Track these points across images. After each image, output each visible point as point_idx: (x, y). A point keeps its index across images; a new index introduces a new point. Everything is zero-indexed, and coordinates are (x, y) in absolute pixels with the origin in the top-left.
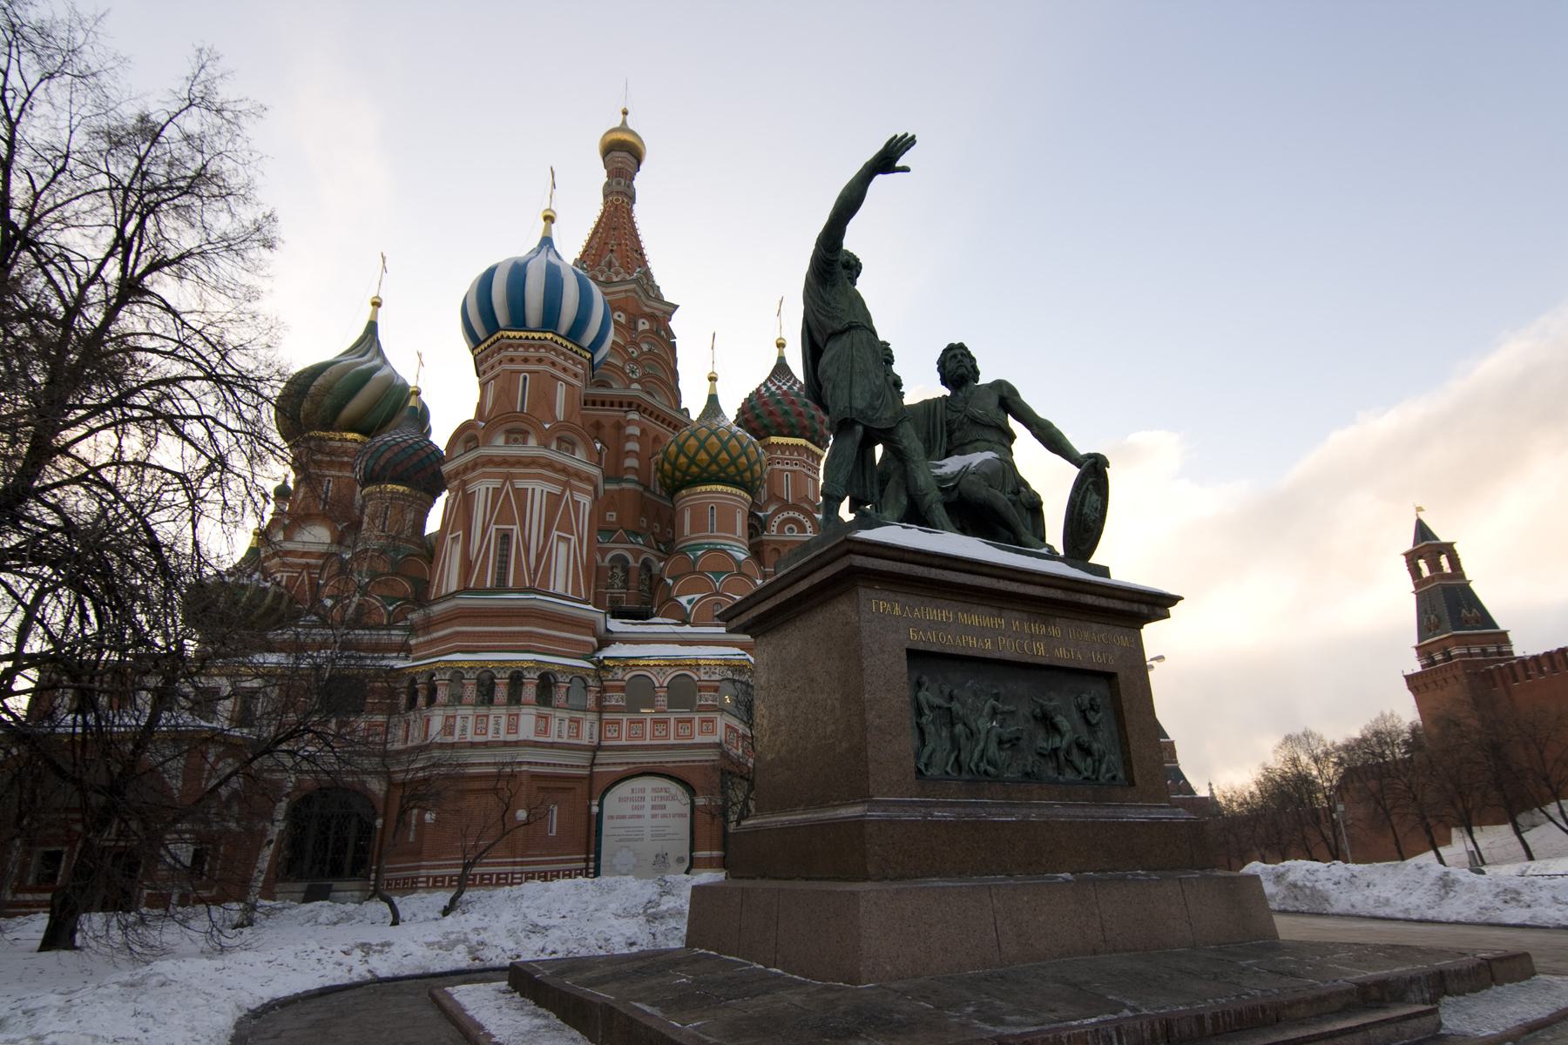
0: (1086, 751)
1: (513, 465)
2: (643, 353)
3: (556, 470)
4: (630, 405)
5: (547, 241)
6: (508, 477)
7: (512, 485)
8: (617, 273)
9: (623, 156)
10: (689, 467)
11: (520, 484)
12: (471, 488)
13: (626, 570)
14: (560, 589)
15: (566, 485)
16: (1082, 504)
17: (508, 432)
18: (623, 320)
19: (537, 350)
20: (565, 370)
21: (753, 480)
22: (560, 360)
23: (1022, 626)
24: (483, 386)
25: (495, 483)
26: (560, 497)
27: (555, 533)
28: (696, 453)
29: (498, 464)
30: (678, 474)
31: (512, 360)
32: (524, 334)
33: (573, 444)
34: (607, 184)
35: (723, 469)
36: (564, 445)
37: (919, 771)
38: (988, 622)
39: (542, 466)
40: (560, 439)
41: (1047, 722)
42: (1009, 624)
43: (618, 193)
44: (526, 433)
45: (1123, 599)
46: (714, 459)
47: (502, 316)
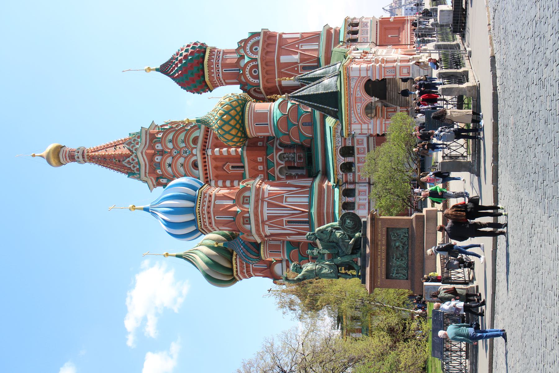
0: (402, 239)
1: (258, 222)
2: (174, 148)
3: (258, 206)
4: (204, 154)
5: (146, 210)
7: (266, 221)
8: (133, 160)
9: (60, 156)
10: (239, 137)
11: (266, 218)
12: (268, 234)
13: (285, 153)
14: (306, 200)
15: (263, 201)
17: (244, 224)
19: (204, 214)
20: (210, 201)
21: (239, 105)
22: (206, 204)
25: (266, 227)
26: (269, 203)
27: (284, 204)
28: (232, 135)
30: (241, 140)
31: (210, 223)
32: (199, 221)
33: (244, 197)
35: (238, 122)
36: (245, 202)
37: (407, 279)
38: (379, 260)
39: (258, 211)
40: (243, 203)
41: (397, 247)
43: (83, 157)
44: (244, 218)
46: (234, 127)
47: (193, 228)
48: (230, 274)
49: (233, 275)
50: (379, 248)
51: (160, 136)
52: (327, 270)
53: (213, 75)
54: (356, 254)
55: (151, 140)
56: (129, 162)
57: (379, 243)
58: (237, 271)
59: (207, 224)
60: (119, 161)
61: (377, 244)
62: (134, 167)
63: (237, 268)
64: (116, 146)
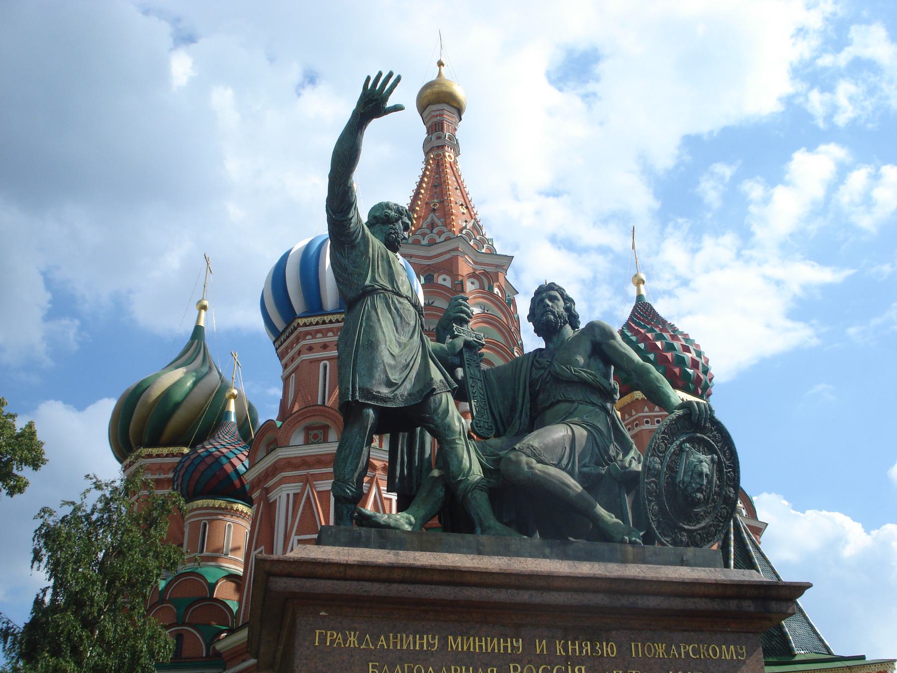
6: (307, 480)
8: (440, 233)
12: (273, 496)
16: (672, 470)
17: (308, 429)
18: (448, 284)
23: (551, 646)
24: (286, 380)
29: (296, 467)
31: (310, 349)
34: (427, 142)
38: (494, 645)
42: (529, 645)
44: (325, 428)
45: (712, 597)
48: (146, 439)
49: (141, 444)
50: (573, 648)
51: (496, 290)
52: (396, 350)
53: (646, 409)
54: (499, 518)
55: (485, 274)
56: (432, 226)
57: (608, 649)
58: (150, 456)
59: (309, 341)
60: (434, 210)
61: (594, 635)
62: (424, 235)
63: (158, 456)
64: (467, 208)
